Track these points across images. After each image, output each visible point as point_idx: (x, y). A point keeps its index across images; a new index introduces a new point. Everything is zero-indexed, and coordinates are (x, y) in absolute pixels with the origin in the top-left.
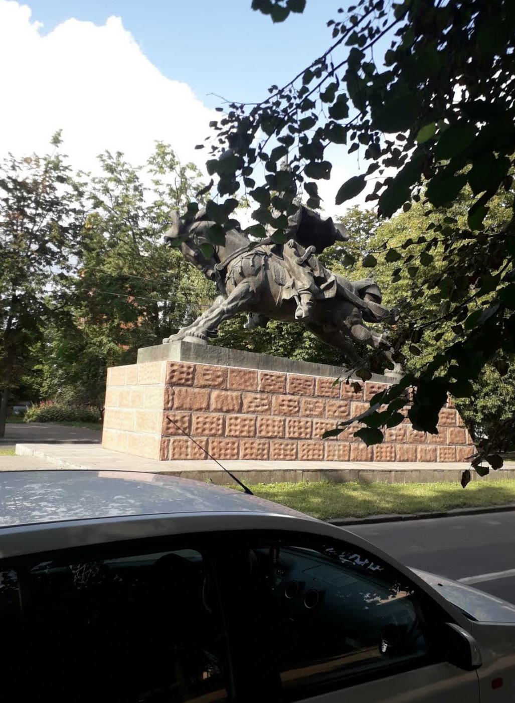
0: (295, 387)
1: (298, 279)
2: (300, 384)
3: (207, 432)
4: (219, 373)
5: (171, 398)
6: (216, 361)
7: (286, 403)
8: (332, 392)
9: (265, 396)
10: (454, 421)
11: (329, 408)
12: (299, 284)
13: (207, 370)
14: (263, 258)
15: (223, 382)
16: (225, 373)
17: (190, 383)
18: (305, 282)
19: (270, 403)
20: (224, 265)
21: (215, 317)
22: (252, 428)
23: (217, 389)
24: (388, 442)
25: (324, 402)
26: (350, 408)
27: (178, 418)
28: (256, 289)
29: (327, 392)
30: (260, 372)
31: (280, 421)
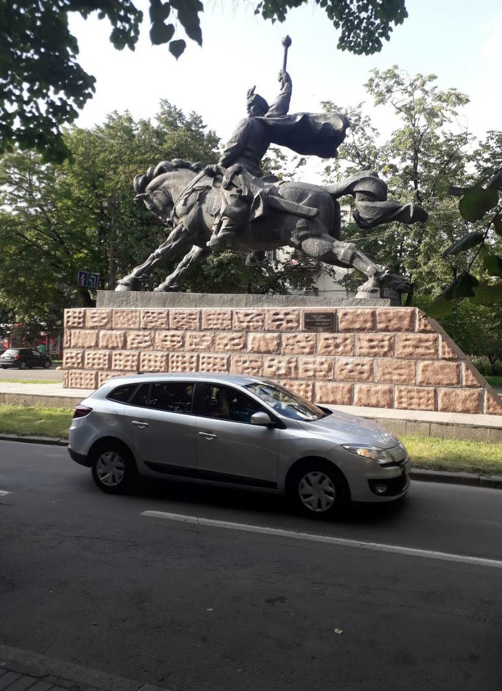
0: (178, 322)
2: (183, 318)
3: (96, 366)
4: (104, 315)
7: (168, 338)
8: (222, 324)
9: (147, 333)
11: (220, 341)
13: (95, 313)
15: (107, 323)
17: (81, 325)
22: (136, 363)
23: (104, 329)
24: (302, 379)
25: (213, 335)
26: (246, 340)
27: (73, 355)
28: (188, 227)
31: (162, 356)
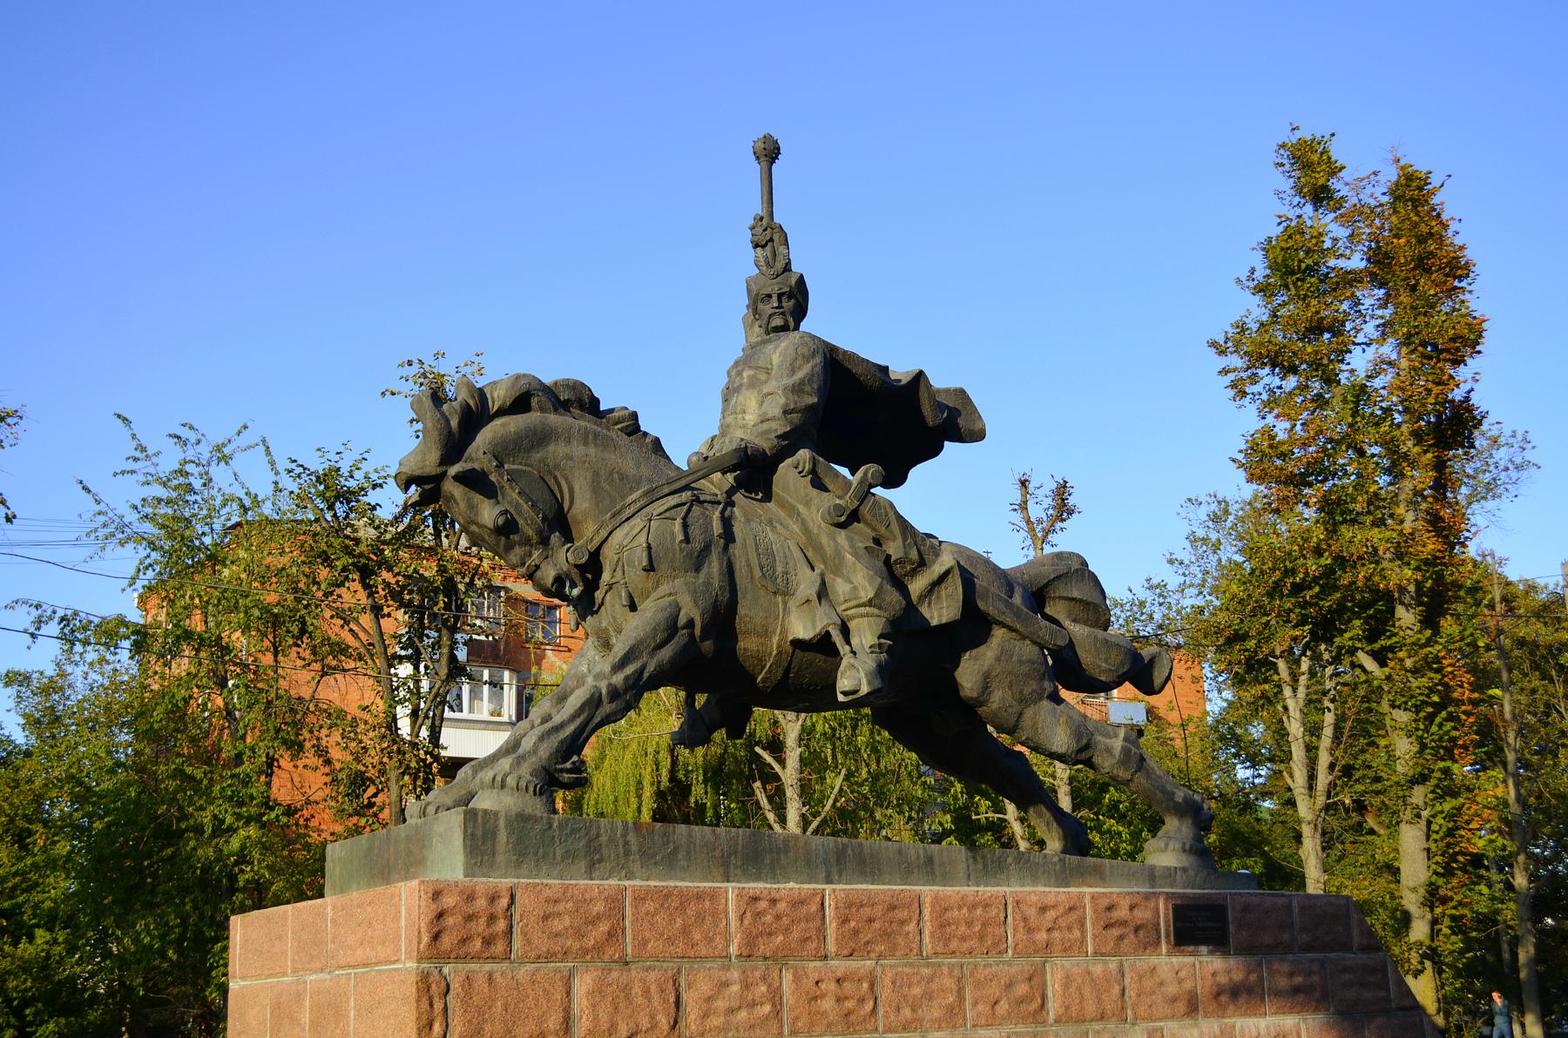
1: (838, 569)
2: (871, 920)
4: (599, 907)
5: (438, 1006)
6: (582, 865)
10: (1383, 994)
12: (840, 588)
14: (717, 514)
15: (610, 934)
16: (615, 903)
18: (857, 582)
19: (775, 997)
20: (592, 547)
21: (573, 718)
29: (963, 939)
30: (731, 889)
